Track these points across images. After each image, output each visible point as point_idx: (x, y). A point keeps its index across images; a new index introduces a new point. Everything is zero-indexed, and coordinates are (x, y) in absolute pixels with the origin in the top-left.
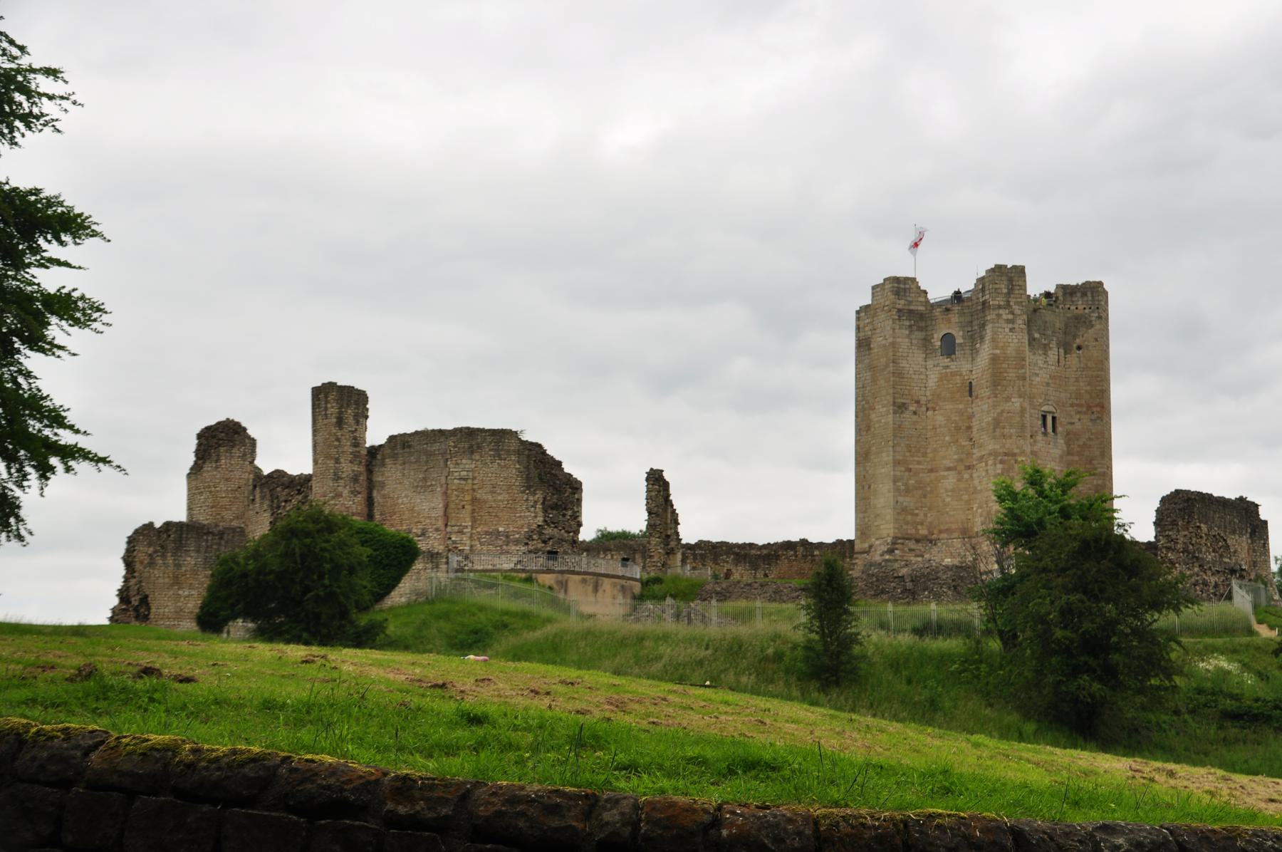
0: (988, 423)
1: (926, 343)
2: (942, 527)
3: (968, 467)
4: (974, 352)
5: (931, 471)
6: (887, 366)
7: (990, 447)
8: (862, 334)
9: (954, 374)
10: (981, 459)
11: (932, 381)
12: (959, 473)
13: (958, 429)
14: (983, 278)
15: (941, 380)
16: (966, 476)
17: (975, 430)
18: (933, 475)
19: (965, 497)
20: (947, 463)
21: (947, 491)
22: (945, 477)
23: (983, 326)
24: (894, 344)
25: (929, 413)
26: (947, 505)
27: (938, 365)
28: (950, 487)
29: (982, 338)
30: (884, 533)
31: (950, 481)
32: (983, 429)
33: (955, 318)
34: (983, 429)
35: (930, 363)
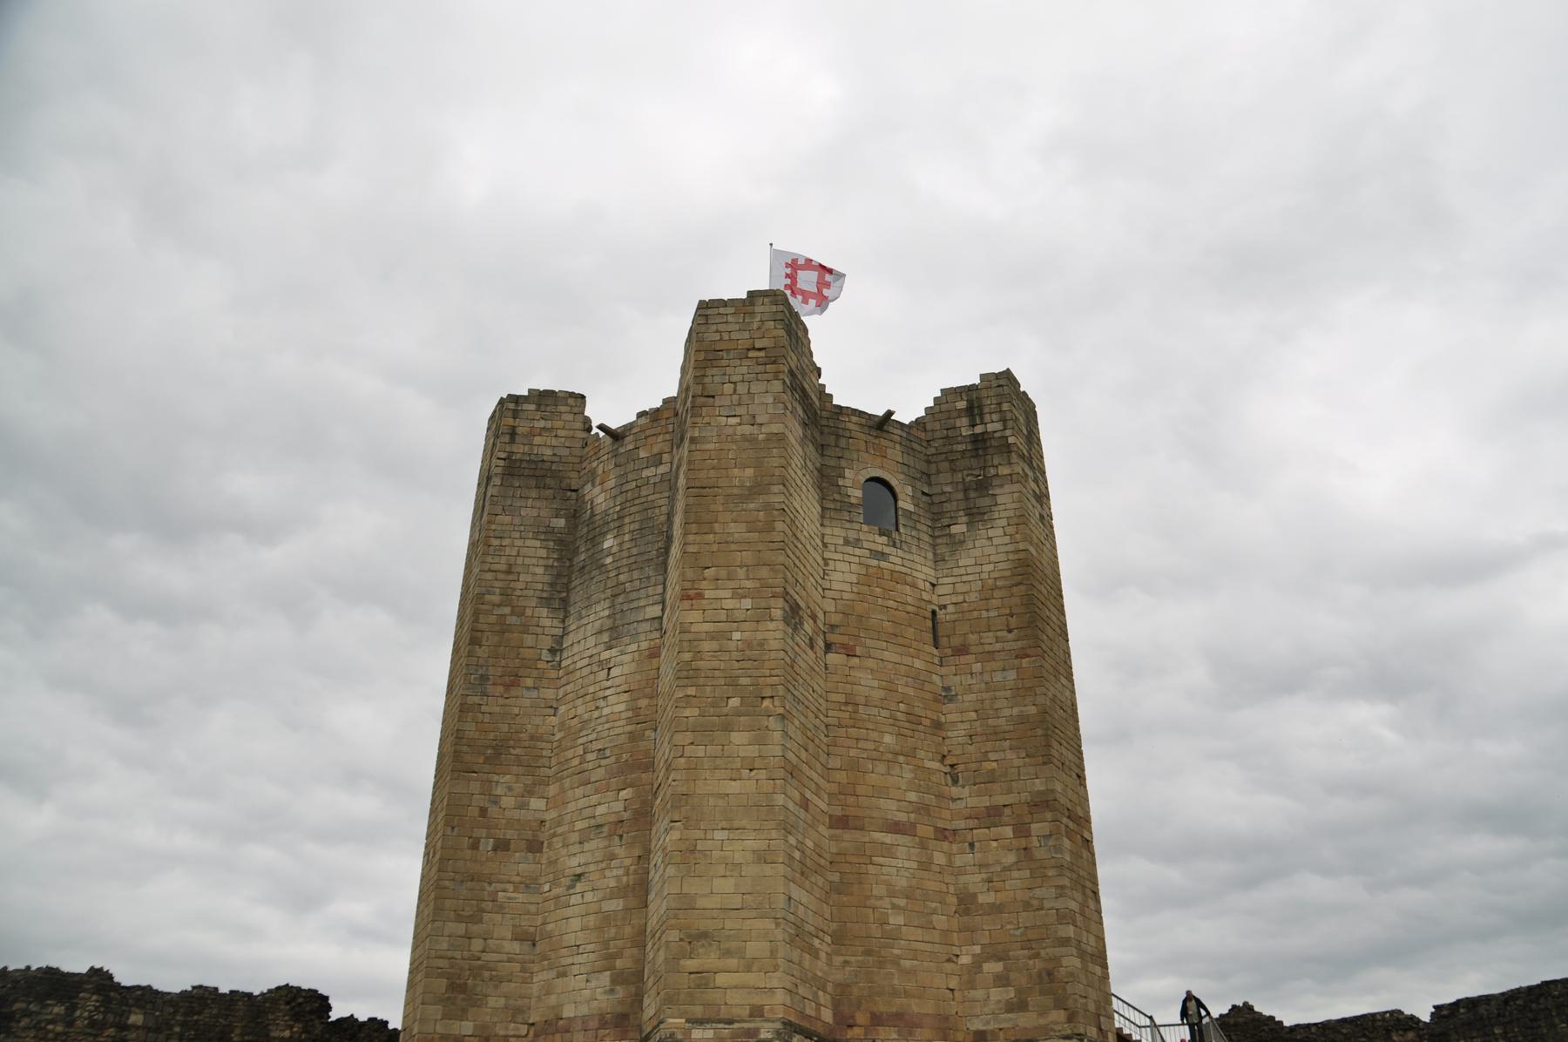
0: (1022, 720)
1: (827, 481)
2: (882, 1007)
3: (942, 834)
4: (943, 545)
5: (841, 822)
6: (758, 488)
7: (1039, 785)
8: (519, 449)
9: (898, 578)
10: (992, 816)
11: (843, 575)
12: (923, 846)
13: (913, 719)
14: (970, 389)
15: (867, 578)
16: (939, 859)
17: (957, 734)
18: (848, 835)
19: (940, 921)
20: (891, 809)
21: (892, 894)
22: (888, 851)
23: (983, 486)
24: (780, 438)
25: (832, 658)
26: (893, 937)
27: (857, 543)
28: (902, 883)
29: (976, 516)
30: (737, 1002)
31: (898, 865)
32: (996, 735)
33: (895, 453)
34: (996, 735)
35: (836, 534)
